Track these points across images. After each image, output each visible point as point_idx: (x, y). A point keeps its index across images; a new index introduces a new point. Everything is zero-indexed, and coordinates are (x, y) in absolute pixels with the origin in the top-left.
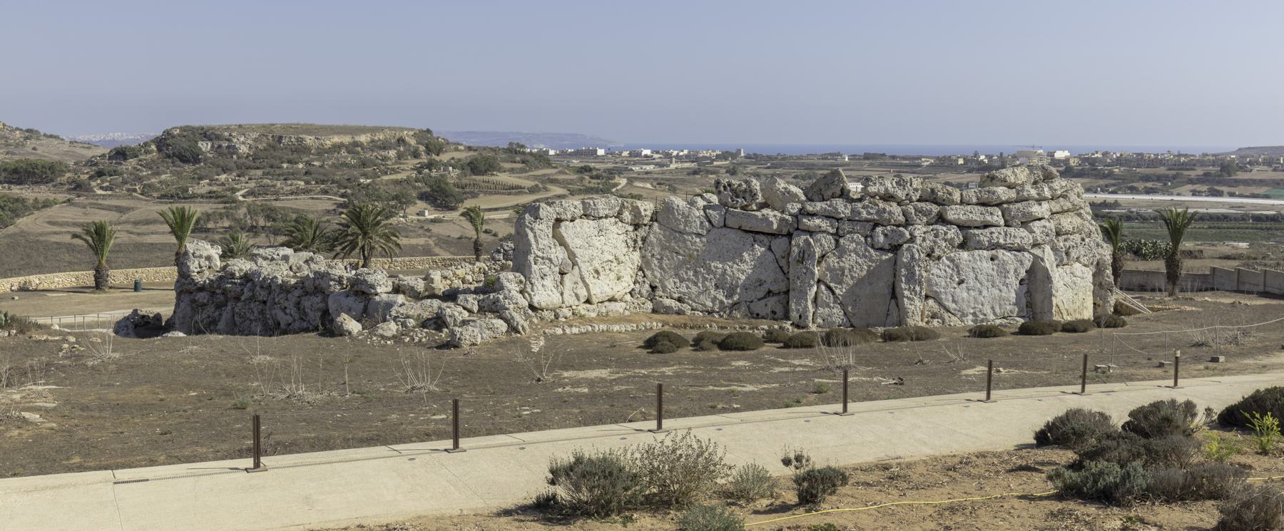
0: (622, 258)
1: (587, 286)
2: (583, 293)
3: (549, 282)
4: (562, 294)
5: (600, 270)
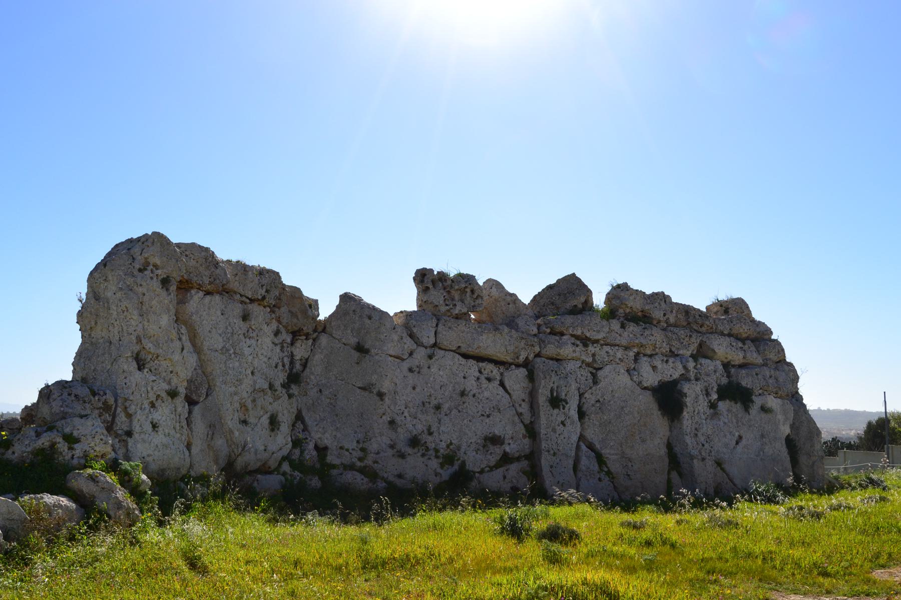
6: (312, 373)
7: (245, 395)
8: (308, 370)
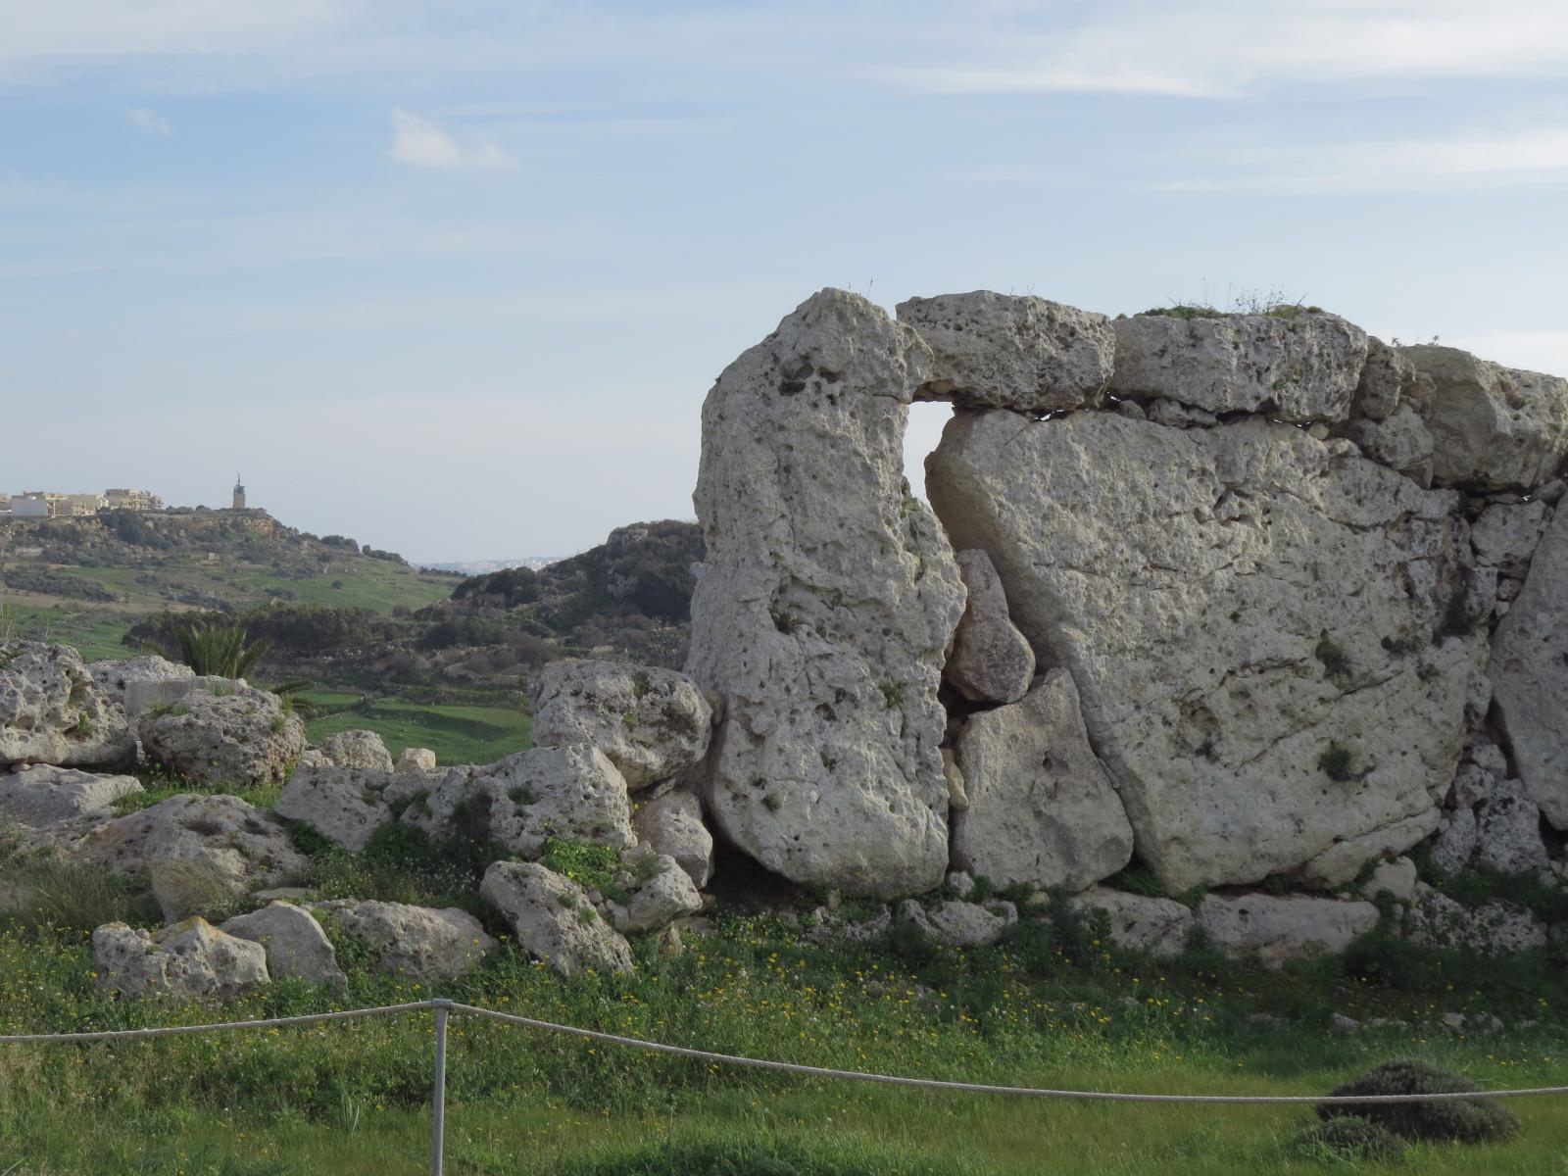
0: (1365, 654)
1: (1127, 789)
2: (1100, 819)
3: (868, 740)
4: (954, 815)
5: (1221, 703)
6: (1544, 607)
7: (1203, 680)
8: (1527, 596)
